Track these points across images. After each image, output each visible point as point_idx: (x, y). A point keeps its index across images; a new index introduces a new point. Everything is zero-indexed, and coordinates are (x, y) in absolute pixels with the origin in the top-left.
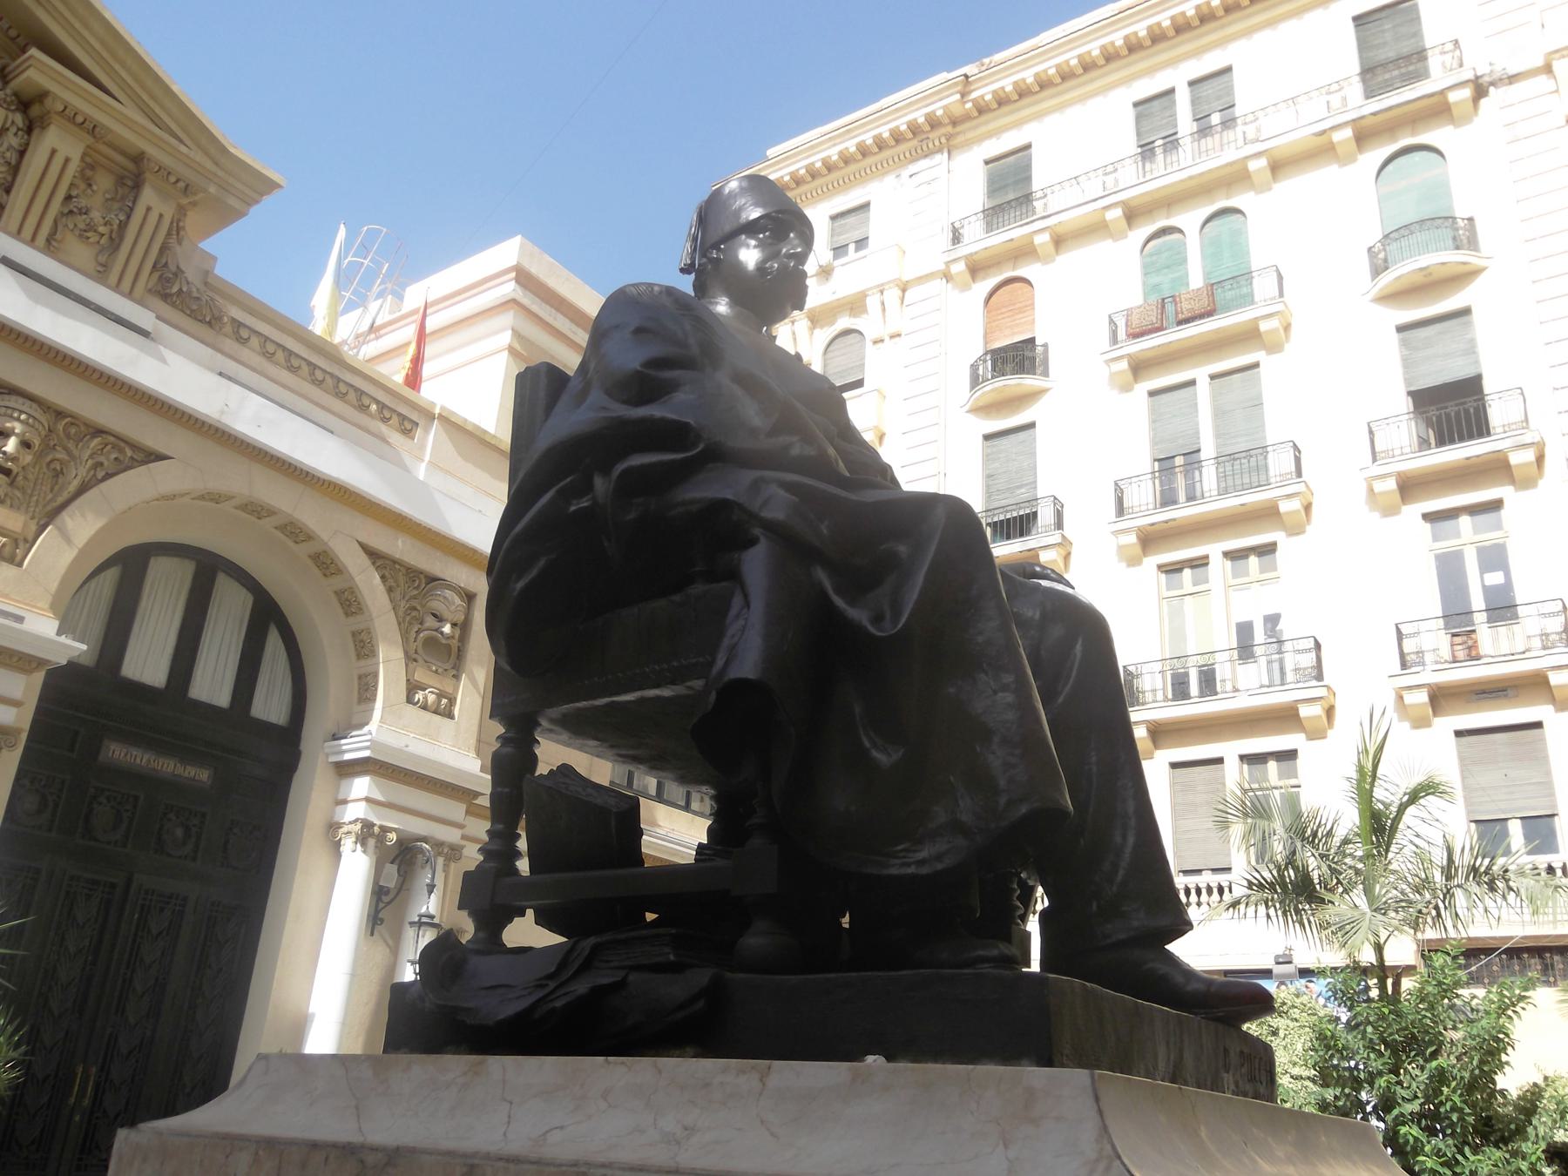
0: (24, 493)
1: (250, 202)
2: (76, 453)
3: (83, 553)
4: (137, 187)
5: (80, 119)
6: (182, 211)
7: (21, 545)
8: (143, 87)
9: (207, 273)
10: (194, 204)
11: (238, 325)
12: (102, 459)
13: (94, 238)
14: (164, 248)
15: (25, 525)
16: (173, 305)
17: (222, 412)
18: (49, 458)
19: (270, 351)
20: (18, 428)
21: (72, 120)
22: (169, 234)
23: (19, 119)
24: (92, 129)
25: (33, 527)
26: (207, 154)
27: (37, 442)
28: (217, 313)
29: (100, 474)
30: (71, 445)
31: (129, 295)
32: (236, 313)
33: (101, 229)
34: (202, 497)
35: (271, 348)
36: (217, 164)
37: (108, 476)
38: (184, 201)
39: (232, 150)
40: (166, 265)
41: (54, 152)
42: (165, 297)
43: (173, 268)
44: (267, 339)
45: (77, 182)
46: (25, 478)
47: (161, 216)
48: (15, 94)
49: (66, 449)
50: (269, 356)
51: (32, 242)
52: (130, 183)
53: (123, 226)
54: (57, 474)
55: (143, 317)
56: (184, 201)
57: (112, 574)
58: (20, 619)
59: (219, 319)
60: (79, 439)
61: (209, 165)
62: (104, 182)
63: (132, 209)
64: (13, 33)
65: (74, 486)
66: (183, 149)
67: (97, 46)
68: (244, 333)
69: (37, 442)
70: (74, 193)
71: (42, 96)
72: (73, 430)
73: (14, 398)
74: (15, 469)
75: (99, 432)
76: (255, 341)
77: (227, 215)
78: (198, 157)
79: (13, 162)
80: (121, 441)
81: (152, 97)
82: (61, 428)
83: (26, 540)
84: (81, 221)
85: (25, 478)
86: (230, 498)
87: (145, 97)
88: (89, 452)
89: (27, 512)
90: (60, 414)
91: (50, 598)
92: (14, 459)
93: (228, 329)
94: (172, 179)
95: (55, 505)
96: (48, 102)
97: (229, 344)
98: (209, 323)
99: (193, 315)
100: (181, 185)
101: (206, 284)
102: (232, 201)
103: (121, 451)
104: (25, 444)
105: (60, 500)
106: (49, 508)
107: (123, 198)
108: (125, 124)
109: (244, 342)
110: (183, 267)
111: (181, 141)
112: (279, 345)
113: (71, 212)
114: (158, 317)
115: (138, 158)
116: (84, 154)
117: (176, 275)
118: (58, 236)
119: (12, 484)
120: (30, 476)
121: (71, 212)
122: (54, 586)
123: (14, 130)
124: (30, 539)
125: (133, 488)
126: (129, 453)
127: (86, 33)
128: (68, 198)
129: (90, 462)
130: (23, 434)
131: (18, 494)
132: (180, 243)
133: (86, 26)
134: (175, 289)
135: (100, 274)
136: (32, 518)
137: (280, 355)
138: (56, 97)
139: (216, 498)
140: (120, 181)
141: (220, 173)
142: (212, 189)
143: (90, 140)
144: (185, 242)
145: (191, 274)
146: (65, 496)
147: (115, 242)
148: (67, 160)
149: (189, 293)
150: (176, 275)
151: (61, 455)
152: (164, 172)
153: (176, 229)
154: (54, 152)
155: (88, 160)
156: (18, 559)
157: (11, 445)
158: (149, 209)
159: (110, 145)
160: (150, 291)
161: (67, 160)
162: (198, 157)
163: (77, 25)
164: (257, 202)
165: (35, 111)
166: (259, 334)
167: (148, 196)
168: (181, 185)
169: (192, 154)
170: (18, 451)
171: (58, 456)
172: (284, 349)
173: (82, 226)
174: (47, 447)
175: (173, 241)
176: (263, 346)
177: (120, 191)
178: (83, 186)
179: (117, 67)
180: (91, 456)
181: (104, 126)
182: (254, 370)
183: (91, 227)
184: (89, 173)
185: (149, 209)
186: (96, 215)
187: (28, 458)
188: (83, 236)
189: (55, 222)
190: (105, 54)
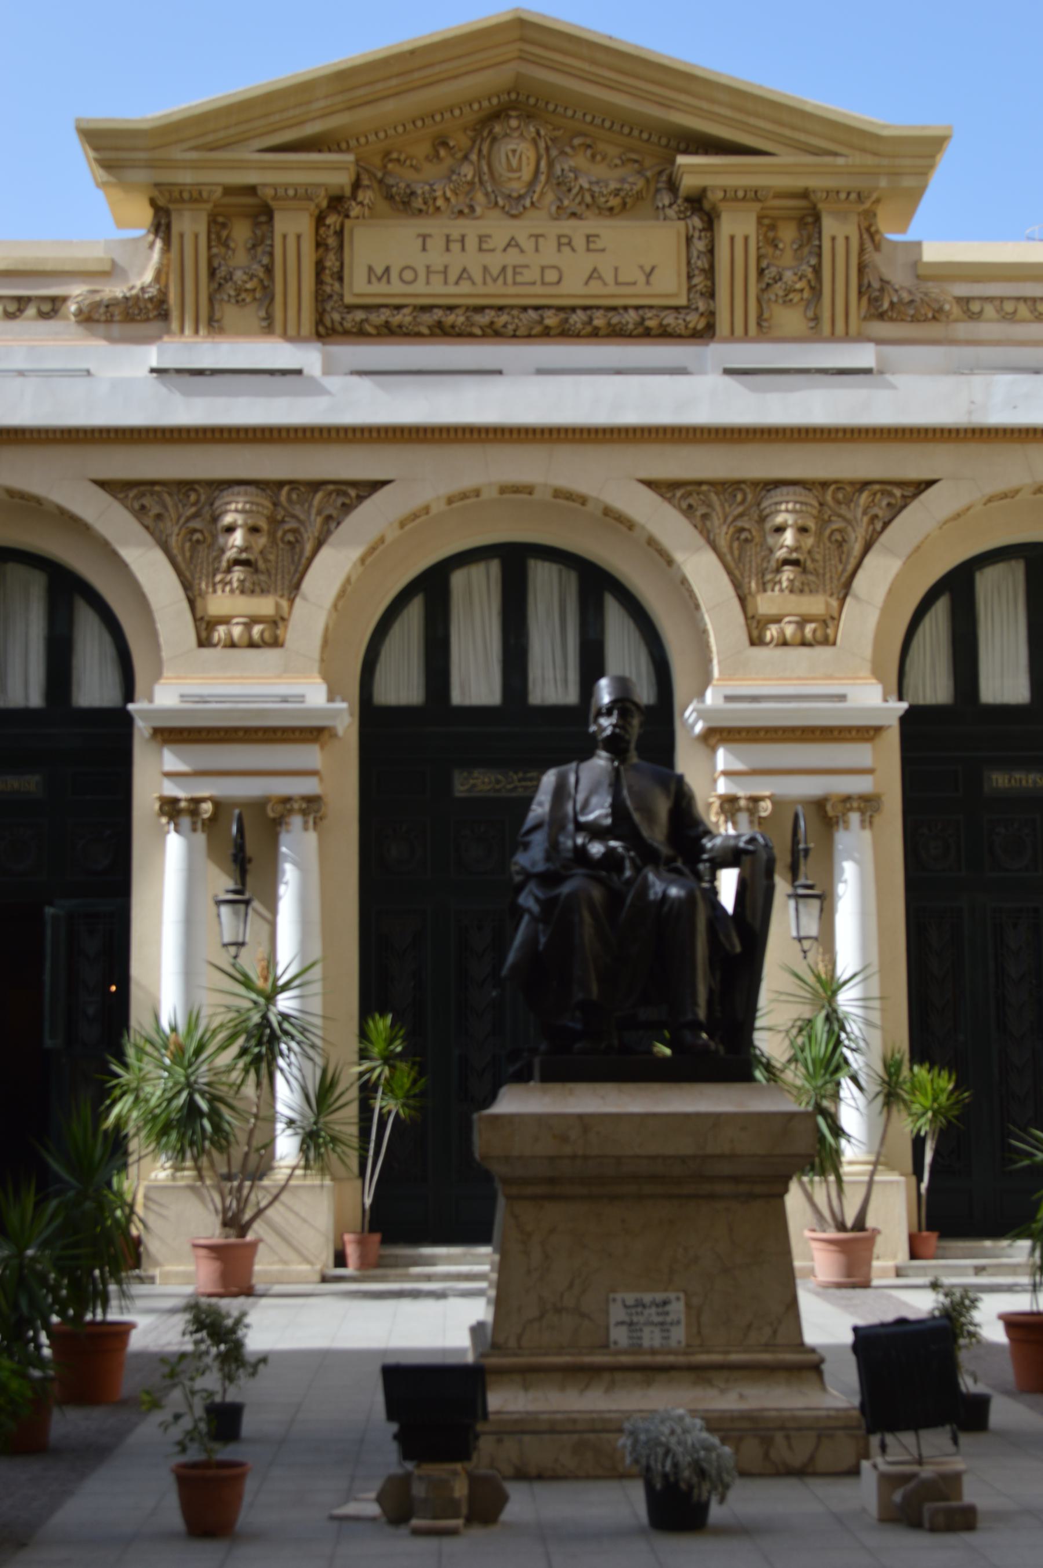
0: (817, 575)
1: (924, 172)
2: (849, 516)
3: (886, 611)
4: (817, 219)
5: (741, 194)
6: (869, 216)
7: (830, 622)
8: (782, 124)
9: (916, 264)
10: (878, 201)
11: (964, 302)
12: (875, 510)
13: (795, 297)
14: (861, 269)
15: (828, 605)
16: (892, 320)
17: (970, 413)
18: (827, 532)
19: (1007, 310)
20: (790, 519)
21: (736, 199)
22: (862, 251)
23: (697, 222)
24: (755, 195)
25: (834, 603)
26: (863, 150)
27: (811, 524)
28: (936, 306)
29: (879, 526)
30: (843, 510)
31: (848, 338)
32: (962, 290)
33: (798, 286)
34: (990, 500)
35: (1009, 307)
36: (876, 154)
37: (886, 525)
38: (867, 205)
39: (885, 133)
40: (869, 285)
41: (732, 238)
42: (881, 316)
43: (876, 285)
44: (1002, 299)
45: (763, 251)
46: (813, 560)
47: (847, 238)
48: (688, 199)
49: (840, 516)
50: (1010, 318)
51: (746, 338)
52: (810, 220)
53: (817, 270)
54: (840, 544)
55: (864, 355)
56: (867, 205)
57: (941, 608)
58: (842, 698)
59: (941, 310)
60: (849, 501)
61: (870, 160)
62: (788, 234)
63: (820, 247)
64: (664, 141)
65: (857, 548)
66: (840, 161)
67: (728, 113)
68: (975, 307)
69: (811, 524)
70: (764, 264)
71: (704, 190)
72: (840, 496)
73: (778, 491)
74: (801, 557)
75: (865, 484)
76: (990, 310)
77: (915, 195)
78: (857, 159)
79: (707, 266)
80: (887, 484)
81: (793, 128)
82: (829, 498)
83: (833, 618)
84: (778, 289)
85: (813, 560)
86: (1017, 492)
87: (787, 132)
88: (859, 511)
89: (825, 591)
90: (824, 484)
91: (868, 666)
92: (796, 549)
93: (956, 311)
94: (843, 196)
95: (847, 574)
96: (709, 194)
97: (963, 329)
98: (934, 318)
99: (914, 319)
100: (853, 196)
101: (918, 277)
102: (908, 182)
103: (891, 494)
104: (803, 530)
105: (850, 568)
106: (843, 579)
107: (810, 239)
108: (780, 172)
109: (974, 317)
110: (888, 275)
111: (835, 154)
112: (1018, 299)
113: (768, 285)
114: (879, 342)
115: (805, 194)
116: (760, 219)
117: (882, 290)
118: (766, 315)
119: (805, 571)
120: (818, 557)
121: (768, 285)
122: (868, 652)
123: (697, 234)
124: (836, 615)
125: (917, 521)
126: (898, 492)
127: (717, 109)
128: (761, 272)
129: (866, 519)
130: (796, 522)
131: (812, 578)
132: (877, 248)
133: (712, 101)
134: (886, 305)
135: (816, 331)
136: (832, 595)
137: (1023, 310)
138: (714, 188)
139: (1004, 496)
140: (801, 223)
141: (885, 162)
142: (883, 183)
143: (759, 205)
144: (884, 247)
145: (899, 278)
146: (853, 562)
147: (816, 290)
148: (746, 239)
149: (901, 300)
150: (882, 290)
151: (837, 524)
152: (832, 194)
153: (870, 234)
154: (732, 238)
155: (766, 221)
156: (831, 638)
157: (789, 537)
158: (833, 239)
159: (780, 195)
160: (865, 319)
161: (746, 239)
162: (857, 159)
163: (705, 105)
164: (931, 167)
165: (707, 206)
166: (989, 299)
167: (830, 226)
168: (853, 196)
169: (850, 161)
170: (797, 540)
171: (834, 526)
172: (1025, 299)
173: (781, 293)
174: (823, 522)
175: (871, 255)
176: (1000, 310)
177: (805, 233)
178: (770, 250)
179: (752, 121)
180: (865, 513)
181: (763, 188)
182: (998, 343)
183: (789, 291)
184: (771, 234)
185: (833, 239)
186: (788, 275)
187: (809, 541)
188: (787, 302)
189: (759, 301)
190: (738, 116)
